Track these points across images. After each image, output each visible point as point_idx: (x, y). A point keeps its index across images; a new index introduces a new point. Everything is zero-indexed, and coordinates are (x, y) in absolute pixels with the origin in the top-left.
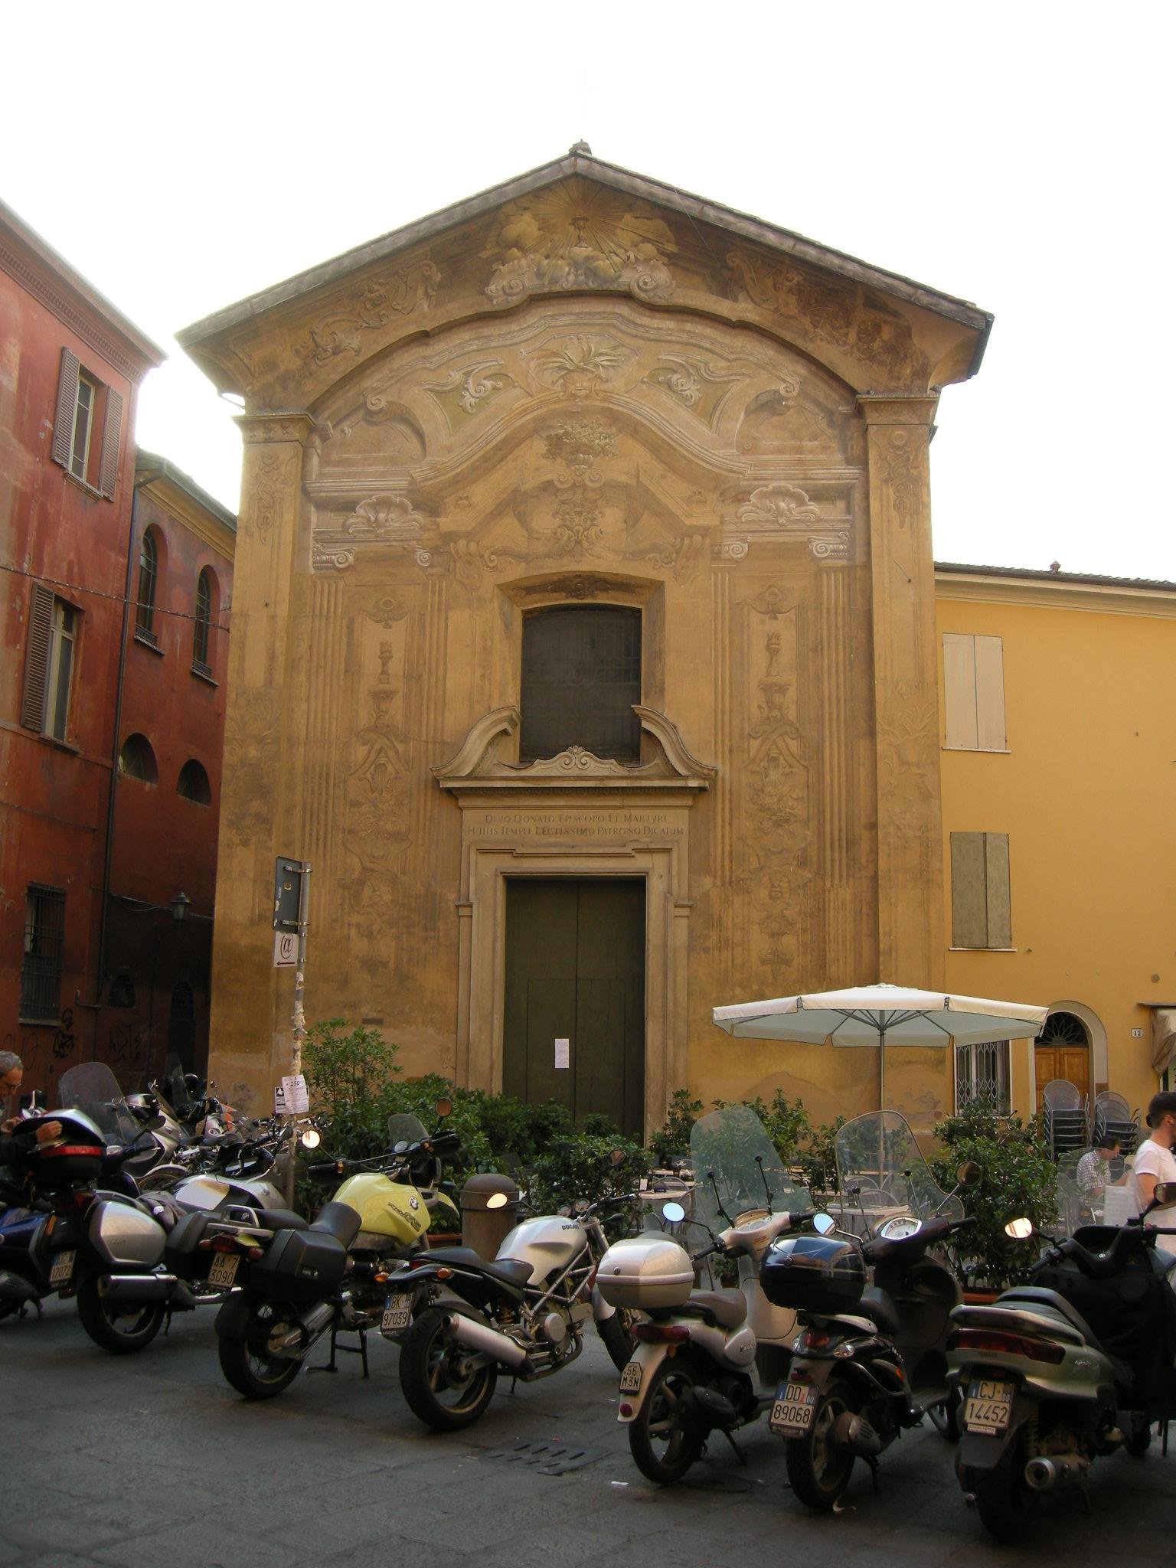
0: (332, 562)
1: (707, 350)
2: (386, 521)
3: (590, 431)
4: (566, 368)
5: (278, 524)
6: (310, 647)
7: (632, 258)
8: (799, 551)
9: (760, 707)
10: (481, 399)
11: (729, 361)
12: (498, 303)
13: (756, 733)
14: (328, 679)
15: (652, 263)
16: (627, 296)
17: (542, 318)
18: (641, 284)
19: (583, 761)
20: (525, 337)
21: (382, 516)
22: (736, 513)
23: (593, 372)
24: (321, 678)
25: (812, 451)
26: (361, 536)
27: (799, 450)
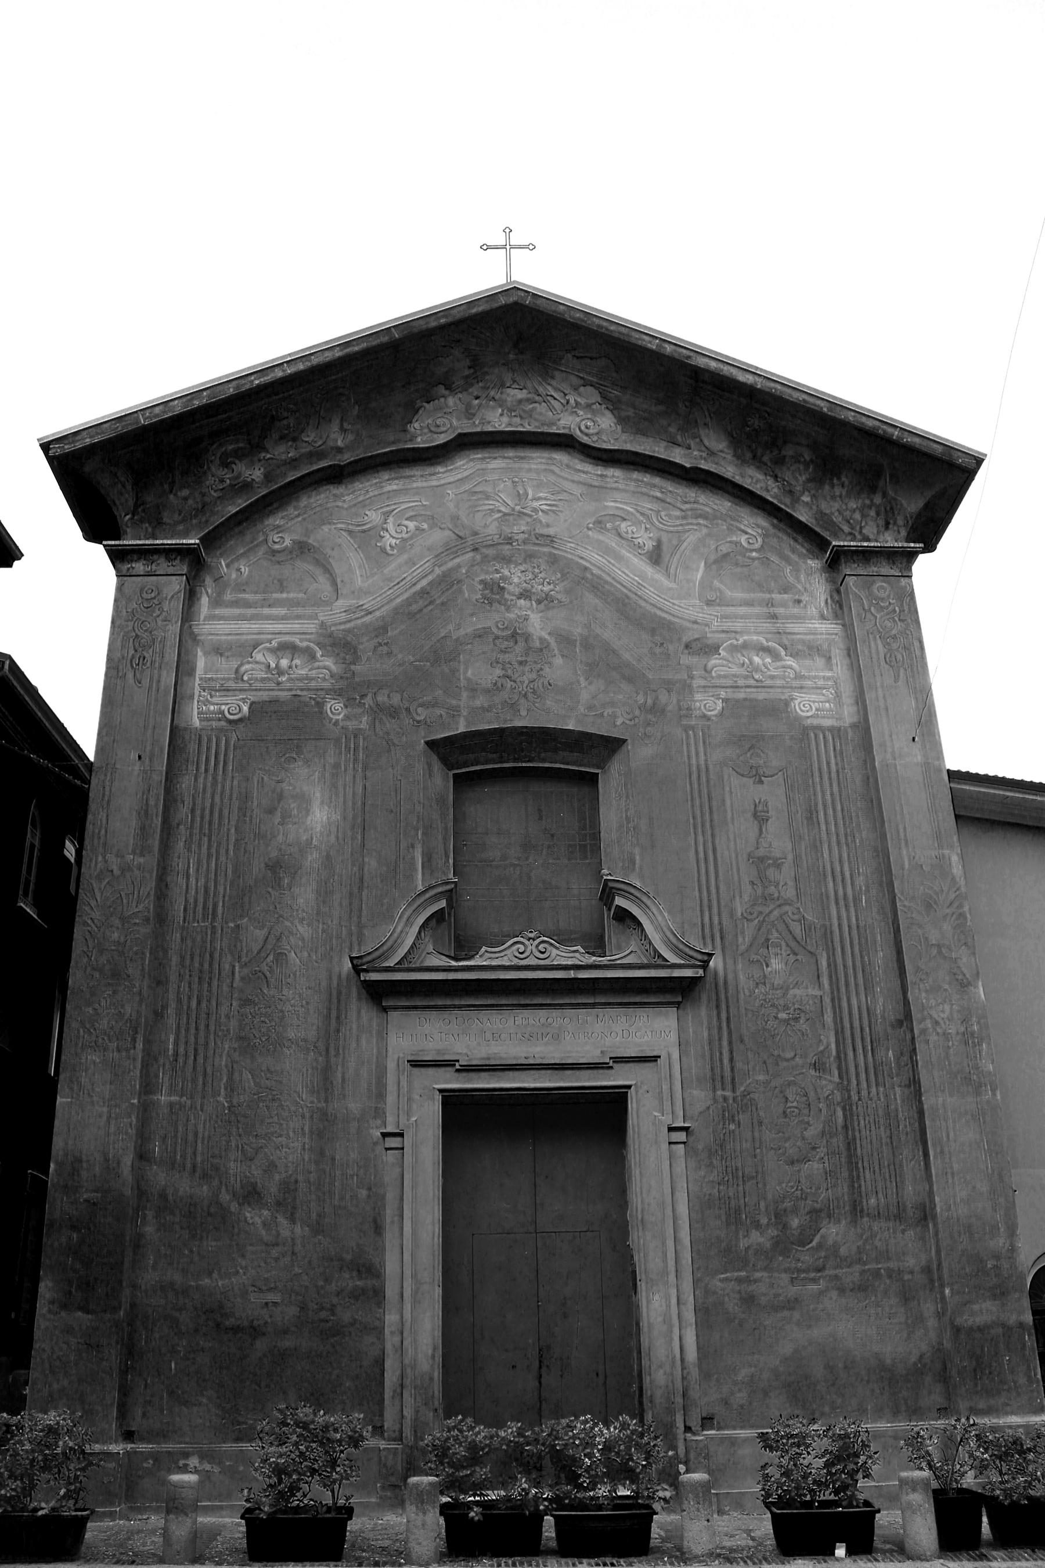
0: (222, 713)
1: (657, 498)
2: (290, 667)
3: (531, 576)
4: (500, 511)
5: (157, 665)
6: (193, 811)
7: (572, 401)
8: (778, 709)
9: (752, 883)
10: (403, 540)
11: (681, 510)
12: (421, 442)
13: (751, 914)
14: (213, 851)
15: (594, 407)
16: (564, 442)
17: (472, 460)
18: (583, 428)
19: (541, 947)
20: (452, 479)
21: (284, 663)
22: (705, 666)
23: (530, 516)
24: (204, 849)
25: (784, 605)
26: (259, 685)
27: (770, 603)
